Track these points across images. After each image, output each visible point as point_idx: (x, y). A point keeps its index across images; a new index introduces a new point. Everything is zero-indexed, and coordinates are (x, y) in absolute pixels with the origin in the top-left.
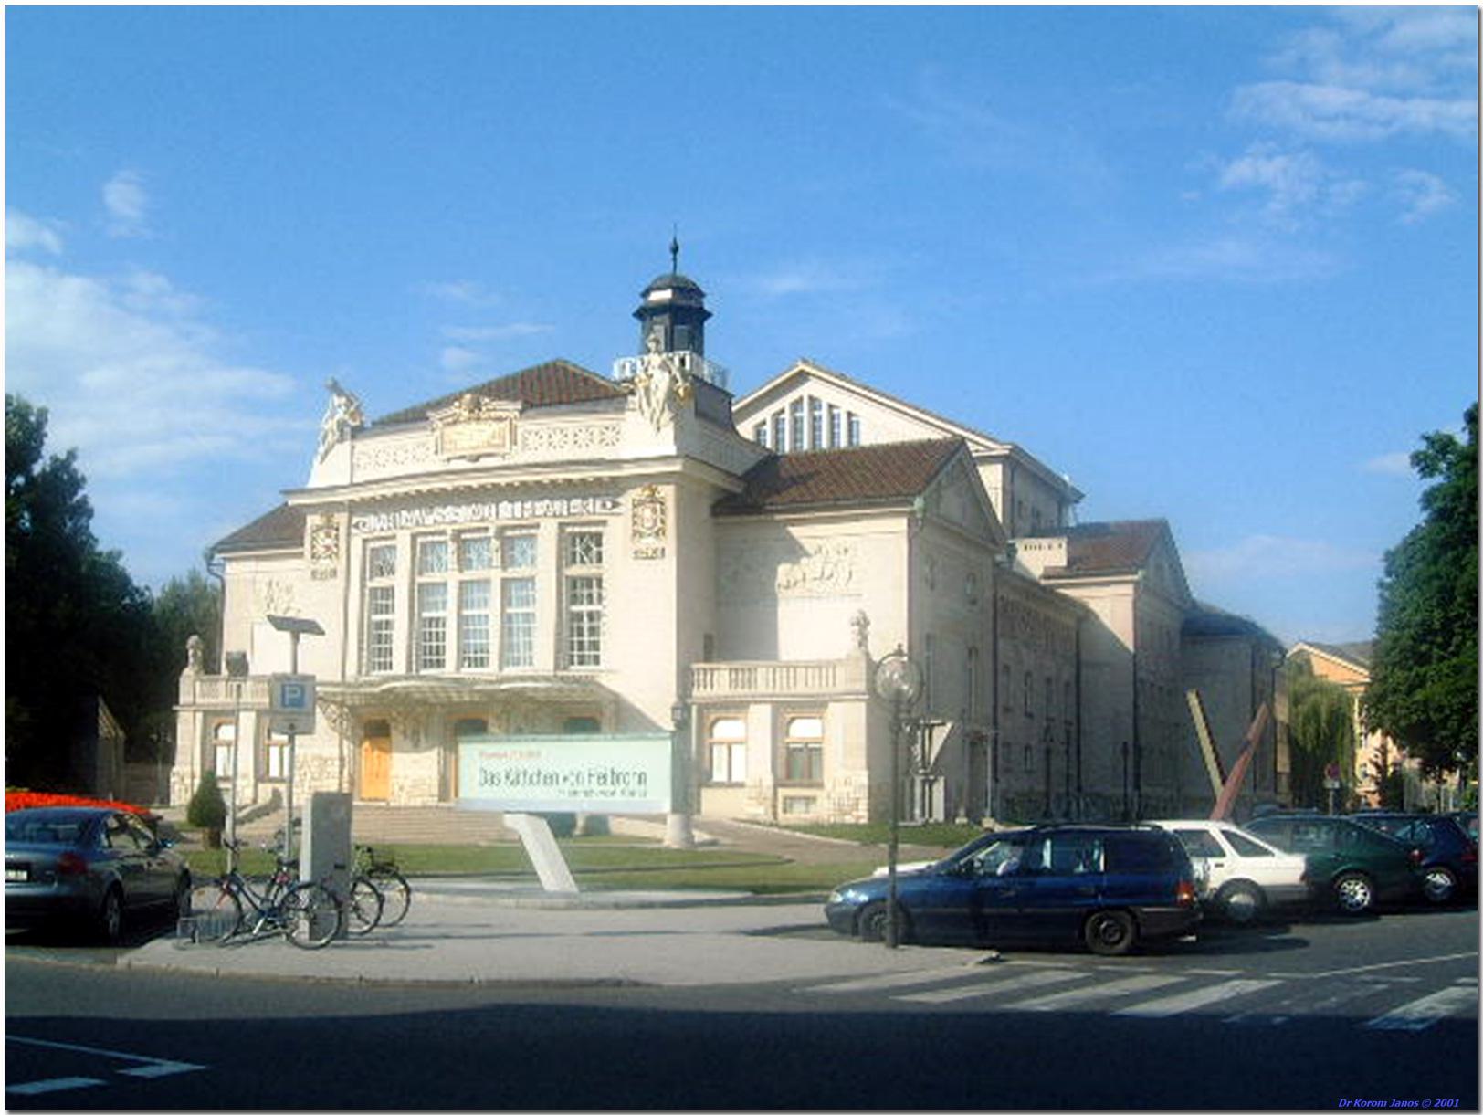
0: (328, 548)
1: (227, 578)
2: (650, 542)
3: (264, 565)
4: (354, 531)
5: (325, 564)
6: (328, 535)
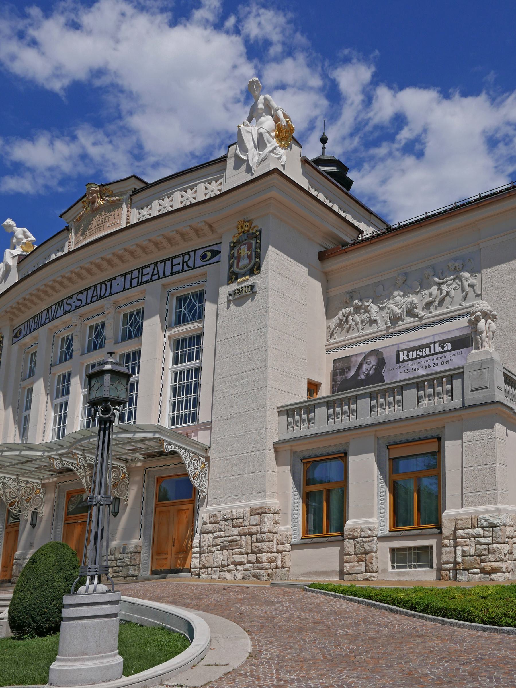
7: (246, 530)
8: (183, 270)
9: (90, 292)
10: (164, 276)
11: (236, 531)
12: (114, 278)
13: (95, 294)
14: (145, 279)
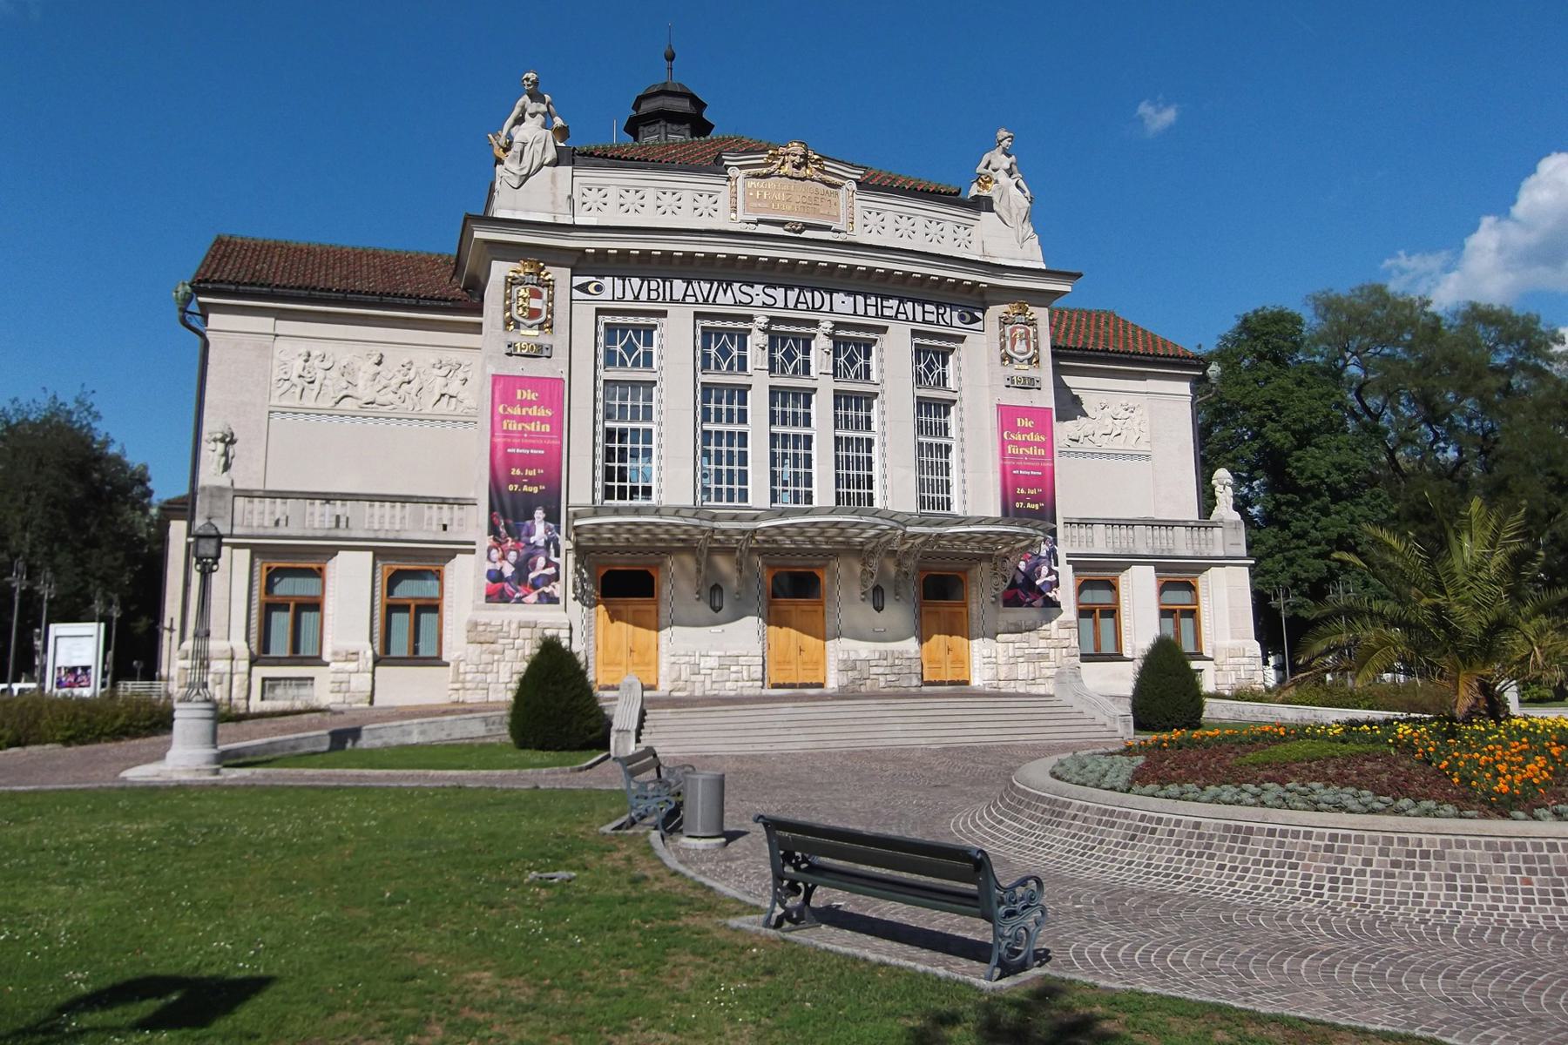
0: (534, 313)
1: (209, 335)
2: (1022, 370)
3: (285, 326)
4: (577, 294)
5: (529, 335)
6: (538, 296)
7: (1055, 643)
8: (938, 323)
9: (792, 295)
10: (914, 320)
11: (1043, 643)
12: (838, 291)
13: (802, 299)
14: (887, 312)
